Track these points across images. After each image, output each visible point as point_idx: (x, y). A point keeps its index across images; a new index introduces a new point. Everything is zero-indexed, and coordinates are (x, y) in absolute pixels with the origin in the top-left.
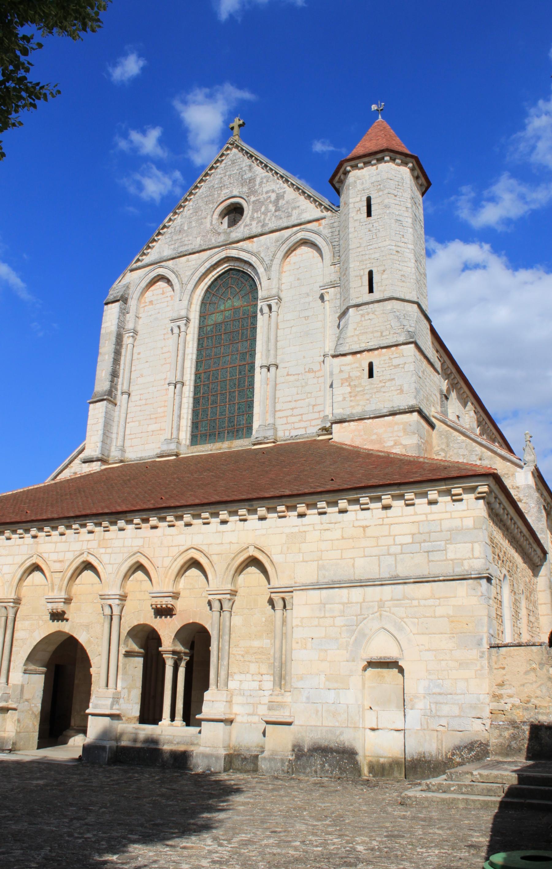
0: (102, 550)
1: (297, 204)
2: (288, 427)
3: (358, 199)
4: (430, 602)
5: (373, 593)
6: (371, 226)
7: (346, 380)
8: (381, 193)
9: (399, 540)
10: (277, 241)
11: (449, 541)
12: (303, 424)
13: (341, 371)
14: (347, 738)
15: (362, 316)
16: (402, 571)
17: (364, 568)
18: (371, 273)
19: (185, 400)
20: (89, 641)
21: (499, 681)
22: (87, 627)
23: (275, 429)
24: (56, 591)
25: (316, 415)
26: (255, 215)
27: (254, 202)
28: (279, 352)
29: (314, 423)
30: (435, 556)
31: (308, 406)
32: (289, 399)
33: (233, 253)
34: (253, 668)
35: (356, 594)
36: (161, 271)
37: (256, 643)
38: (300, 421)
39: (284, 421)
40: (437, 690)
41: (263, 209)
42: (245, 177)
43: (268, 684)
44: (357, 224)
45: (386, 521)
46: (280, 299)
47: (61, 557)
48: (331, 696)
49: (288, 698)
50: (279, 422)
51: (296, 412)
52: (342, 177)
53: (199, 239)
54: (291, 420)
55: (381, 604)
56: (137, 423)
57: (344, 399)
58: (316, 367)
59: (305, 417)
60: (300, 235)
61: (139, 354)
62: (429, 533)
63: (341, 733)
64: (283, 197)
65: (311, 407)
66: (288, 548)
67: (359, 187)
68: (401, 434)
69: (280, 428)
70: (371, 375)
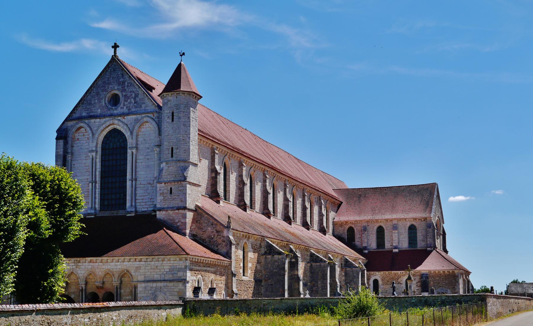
2: (141, 207)
3: (168, 112)
5: (159, 284)
9: (166, 270)
11: (178, 271)
12: (146, 206)
13: (160, 190)
15: (169, 167)
16: (166, 278)
17: (157, 277)
18: (172, 148)
19: (97, 190)
20: (75, 298)
22: (74, 293)
23: (136, 208)
25: (152, 203)
28: (137, 173)
30: (174, 275)
32: (141, 195)
35: (154, 285)
38: (146, 205)
39: (139, 204)
41: (129, 101)
44: (168, 124)
46: (137, 148)
50: (137, 204)
51: (144, 201)
55: (161, 287)
58: (152, 182)
59: (147, 204)
60: (145, 119)
64: (138, 97)
67: (169, 105)
68: (181, 217)
69: (138, 207)
70: (171, 193)
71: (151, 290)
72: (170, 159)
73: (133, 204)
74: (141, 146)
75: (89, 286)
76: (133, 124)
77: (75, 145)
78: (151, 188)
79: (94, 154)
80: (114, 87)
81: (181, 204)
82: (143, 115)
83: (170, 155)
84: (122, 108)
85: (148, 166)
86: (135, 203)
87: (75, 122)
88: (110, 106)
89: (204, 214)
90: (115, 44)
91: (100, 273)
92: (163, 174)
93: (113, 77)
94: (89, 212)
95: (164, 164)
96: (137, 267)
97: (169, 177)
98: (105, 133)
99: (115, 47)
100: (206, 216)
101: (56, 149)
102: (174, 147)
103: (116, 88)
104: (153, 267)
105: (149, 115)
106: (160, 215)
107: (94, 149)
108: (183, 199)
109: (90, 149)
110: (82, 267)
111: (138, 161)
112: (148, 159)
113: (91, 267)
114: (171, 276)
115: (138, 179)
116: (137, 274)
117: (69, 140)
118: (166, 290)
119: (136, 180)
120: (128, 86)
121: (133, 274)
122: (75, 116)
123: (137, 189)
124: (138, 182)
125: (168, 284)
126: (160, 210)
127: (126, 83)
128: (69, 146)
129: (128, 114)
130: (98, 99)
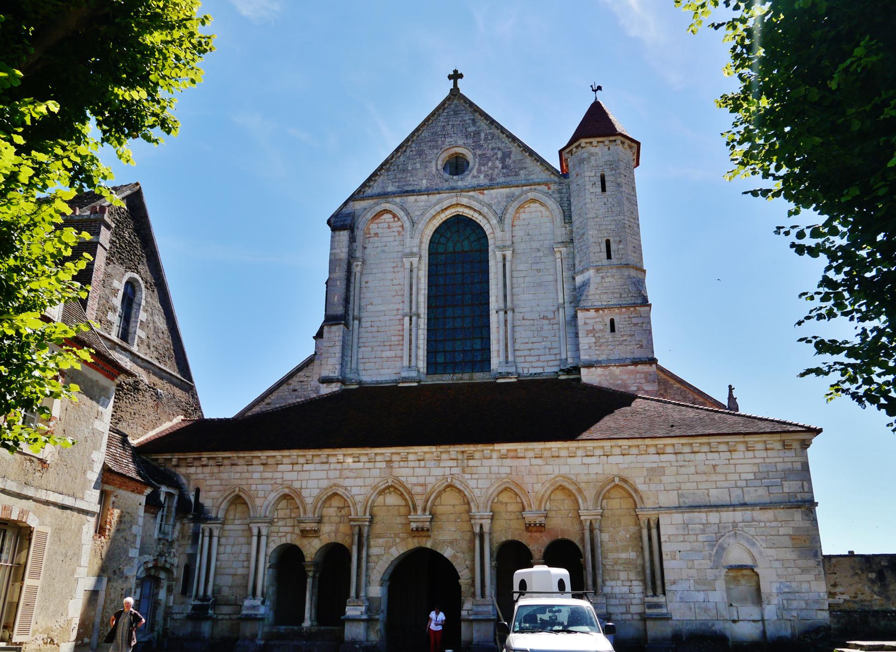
0: (468, 476)
1: (524, 165)
2: (527, 365)
3: (593, 174)
4: (774, 524)
5: (728, 516)
6: (605, 200)
7: (591, 331)
8: (613, 172)
9: (744, 476)
10: (508, 197)
12: (540, 364)
13: (586, 323)
14: (718, 626)
15: (602, 278)
16: (748, 499)
17: (716, 496)
18: (608, 243)
19: (421, 332)
20: (455, 556)
21: (833, 583)
22: (452, 543)
24: (419, 512)
25: (553, 357)
26: (483, 168)
27: (480, 155)
28: (515, 298)
29: (551, 363)
31: (545, 348)
32: (526, 340)
33: (465, 201)
34: (623, 575)
35: (714, 517)
36: (388, 206)
37: (623, 556)
38: (538, 361)
39: (522, 359)
40: (786, 590)
41: (490, 164)
42: (469, 130)
43: (638, 588)
44: (593, 196)
45: (732, 462)
47: (421, 480)
48: (701, 596)
49: (661, 599)
50: (518, 360)
52: (574, 150)
53: (424, 181)
54: (531, 359)
55: (735, 525)
56: (370, 349)
57: (590, 348)
58: (550, 315)
59: (542, 358)
60: (531, 195)
61: (367, 282)
62: (768, 472)
63: (713, 625)
65: (547, 350)
66: (650, 480)
67: (593, 162)
68: (643, 381)
69: (519, 365)
70: (613, 329)
71: (703, 531)
72: (605, 262)
73: (510, 358)
74: (520, 247)
75: (500, 524)
76: (504, 204)
77: (369, 246)
78: (550, 327)
79: (415, 260)
80: (456, 142)
81: (639, 354)
82: (525, 188)
83: (605, 255)
84: (474, 177)
85: (540, 285)
86: (515, 357)
87: (371, 202)
88: (446, 176)
89: (672, 381)
90: (456, 71)
91: (538, 487)
92: (591, 293)
93: (453, 126)
94: (404, 374)
95: (592, 272)
96: (651, 470)
97: (604, 297)
98: (437, 222)
99: (456, 76)
100: (678, 385)
101: (332, 248)
102: (612, 240)
103: (460, 142)
104: (702, 468)
105: (539, 187)
106: (588, 376)
107: (415, 250)
108: (644, 343)
109: (407, 250)
110: (481, 470)
111: (515, 274)
112: (539, 271)
113: (508, 470)
114: (762, 492)
115: (516, 310)
116: (652, 487)
117: (359, 234)
118: (752, 531)
119: (513, 310)
120: (486, 139)
121: (641, 487)
122: (369, 191)
123: (517, 329)
124: (518, 316)
125: (758, 514)
126: (589, 365)
127: (483, 135)
128: (358, 244)
129: (491, 187)
130: (422, 162)
